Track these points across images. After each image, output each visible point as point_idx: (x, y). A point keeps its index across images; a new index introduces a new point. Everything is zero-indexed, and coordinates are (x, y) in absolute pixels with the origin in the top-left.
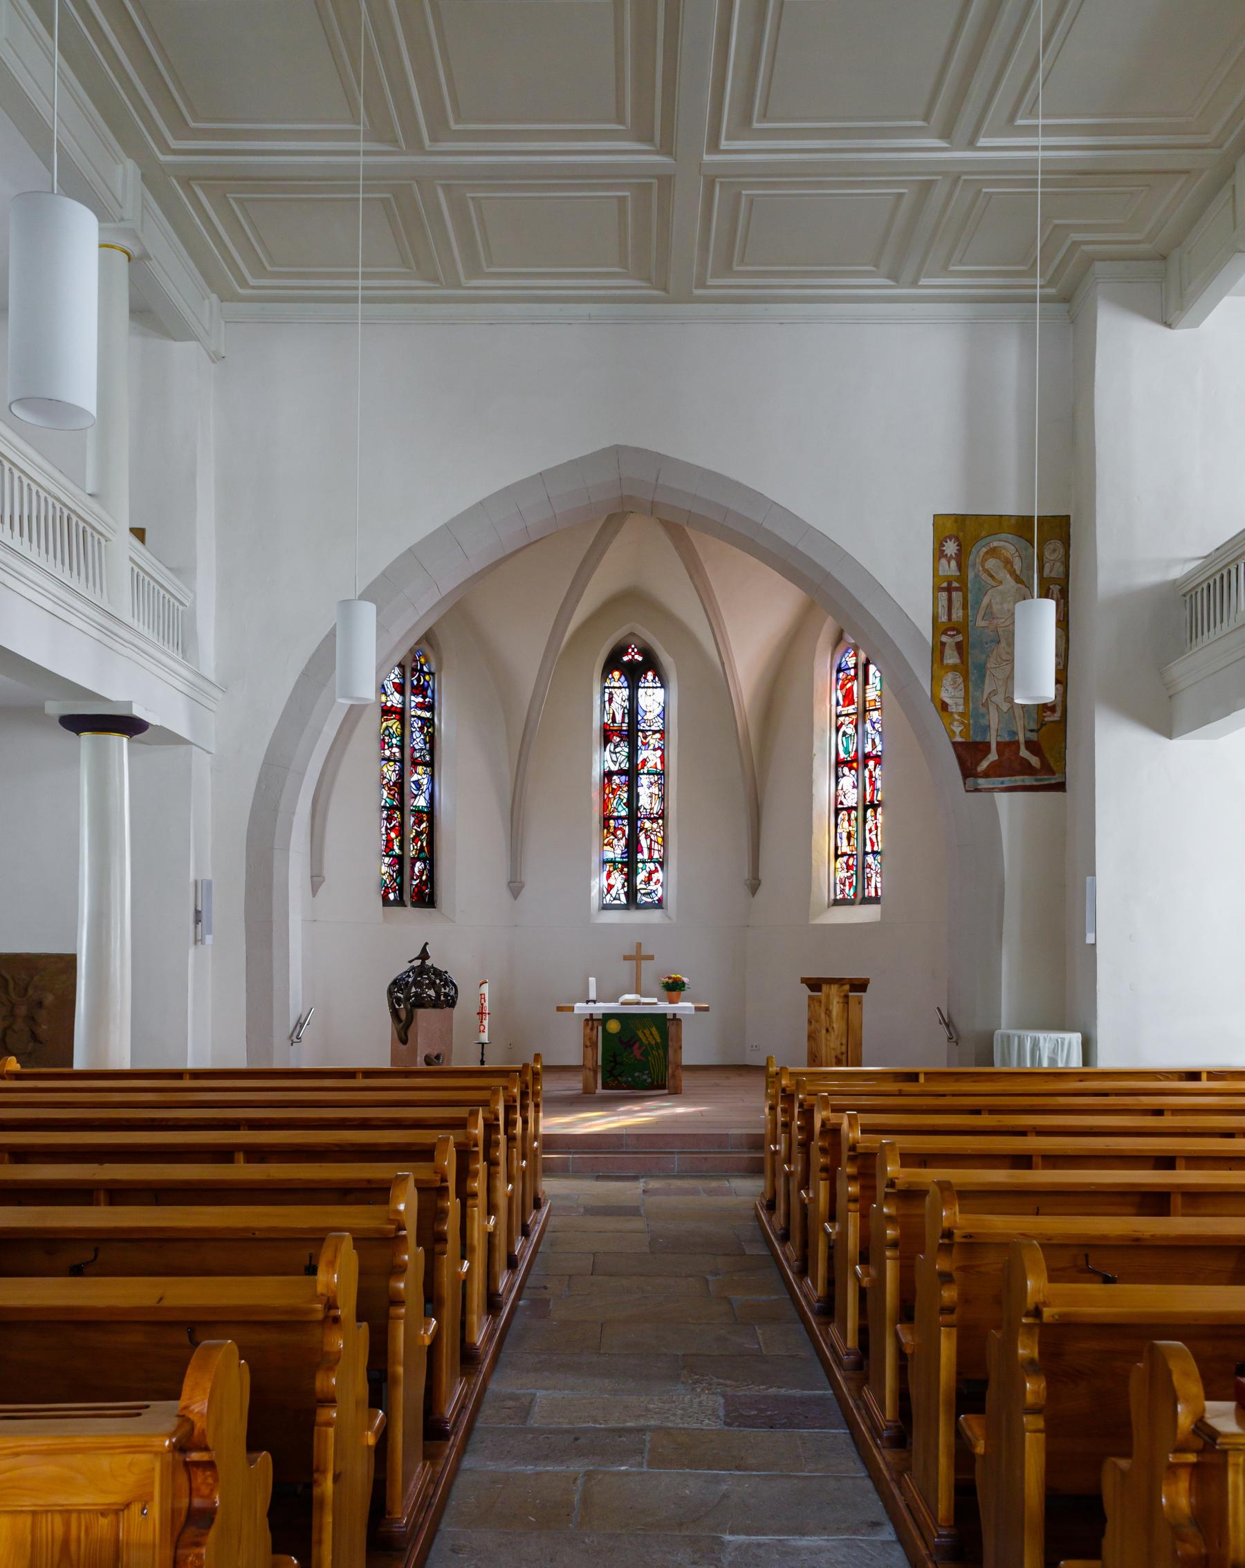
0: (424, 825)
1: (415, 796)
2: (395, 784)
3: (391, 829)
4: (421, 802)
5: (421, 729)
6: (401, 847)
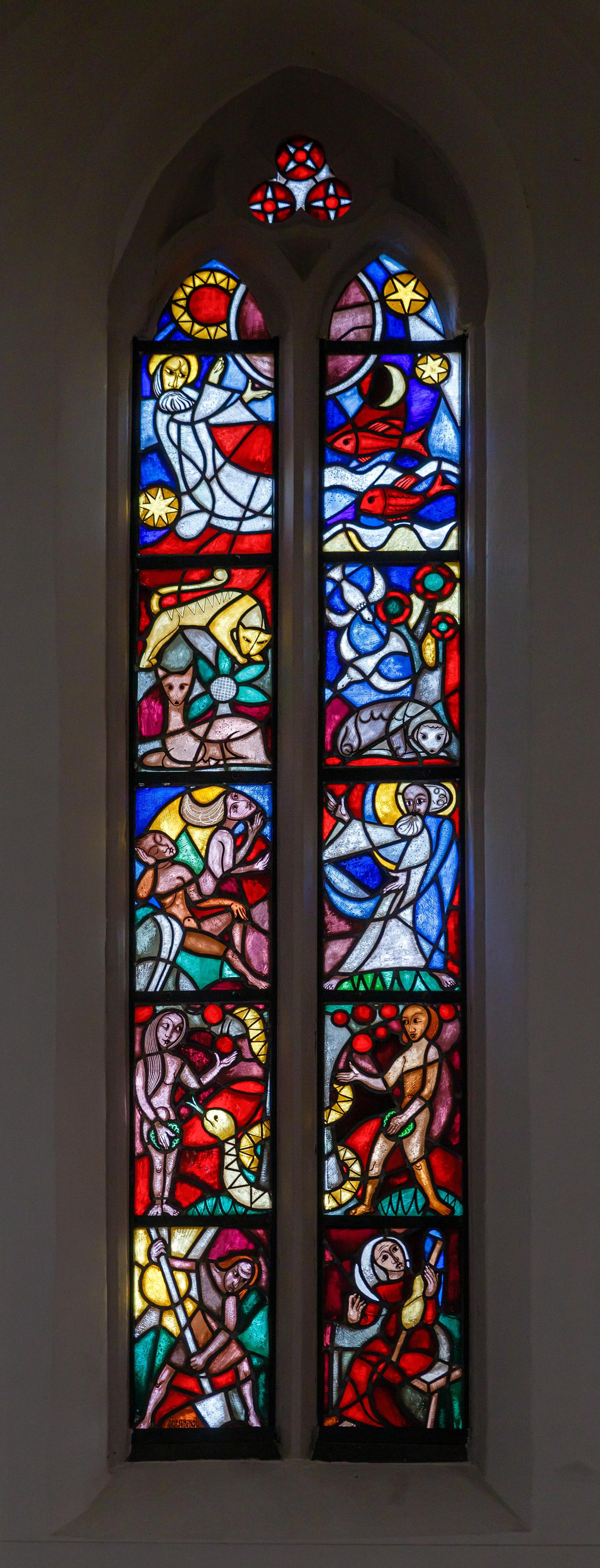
0: (413, 1057)
1: (357, 928)
2: (229, 885)
3: (208, 1096)
4: (396, 949)
5: (387, 616)
6: (271, 1173)
